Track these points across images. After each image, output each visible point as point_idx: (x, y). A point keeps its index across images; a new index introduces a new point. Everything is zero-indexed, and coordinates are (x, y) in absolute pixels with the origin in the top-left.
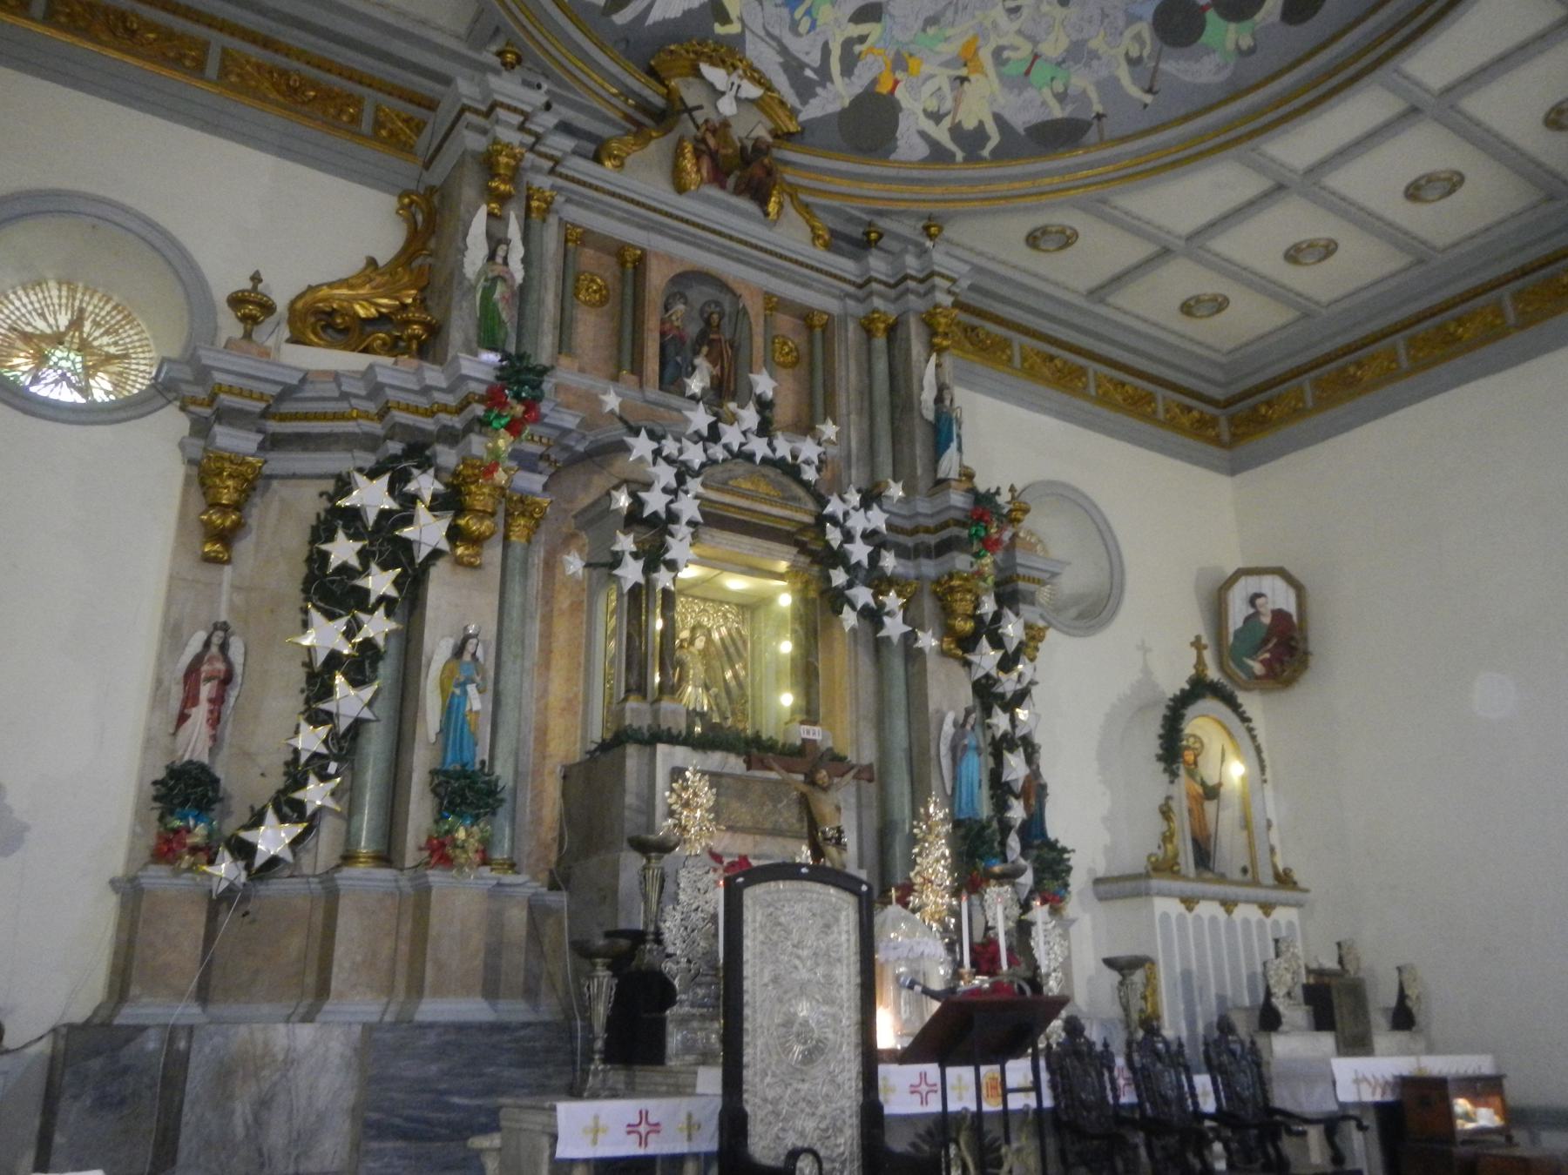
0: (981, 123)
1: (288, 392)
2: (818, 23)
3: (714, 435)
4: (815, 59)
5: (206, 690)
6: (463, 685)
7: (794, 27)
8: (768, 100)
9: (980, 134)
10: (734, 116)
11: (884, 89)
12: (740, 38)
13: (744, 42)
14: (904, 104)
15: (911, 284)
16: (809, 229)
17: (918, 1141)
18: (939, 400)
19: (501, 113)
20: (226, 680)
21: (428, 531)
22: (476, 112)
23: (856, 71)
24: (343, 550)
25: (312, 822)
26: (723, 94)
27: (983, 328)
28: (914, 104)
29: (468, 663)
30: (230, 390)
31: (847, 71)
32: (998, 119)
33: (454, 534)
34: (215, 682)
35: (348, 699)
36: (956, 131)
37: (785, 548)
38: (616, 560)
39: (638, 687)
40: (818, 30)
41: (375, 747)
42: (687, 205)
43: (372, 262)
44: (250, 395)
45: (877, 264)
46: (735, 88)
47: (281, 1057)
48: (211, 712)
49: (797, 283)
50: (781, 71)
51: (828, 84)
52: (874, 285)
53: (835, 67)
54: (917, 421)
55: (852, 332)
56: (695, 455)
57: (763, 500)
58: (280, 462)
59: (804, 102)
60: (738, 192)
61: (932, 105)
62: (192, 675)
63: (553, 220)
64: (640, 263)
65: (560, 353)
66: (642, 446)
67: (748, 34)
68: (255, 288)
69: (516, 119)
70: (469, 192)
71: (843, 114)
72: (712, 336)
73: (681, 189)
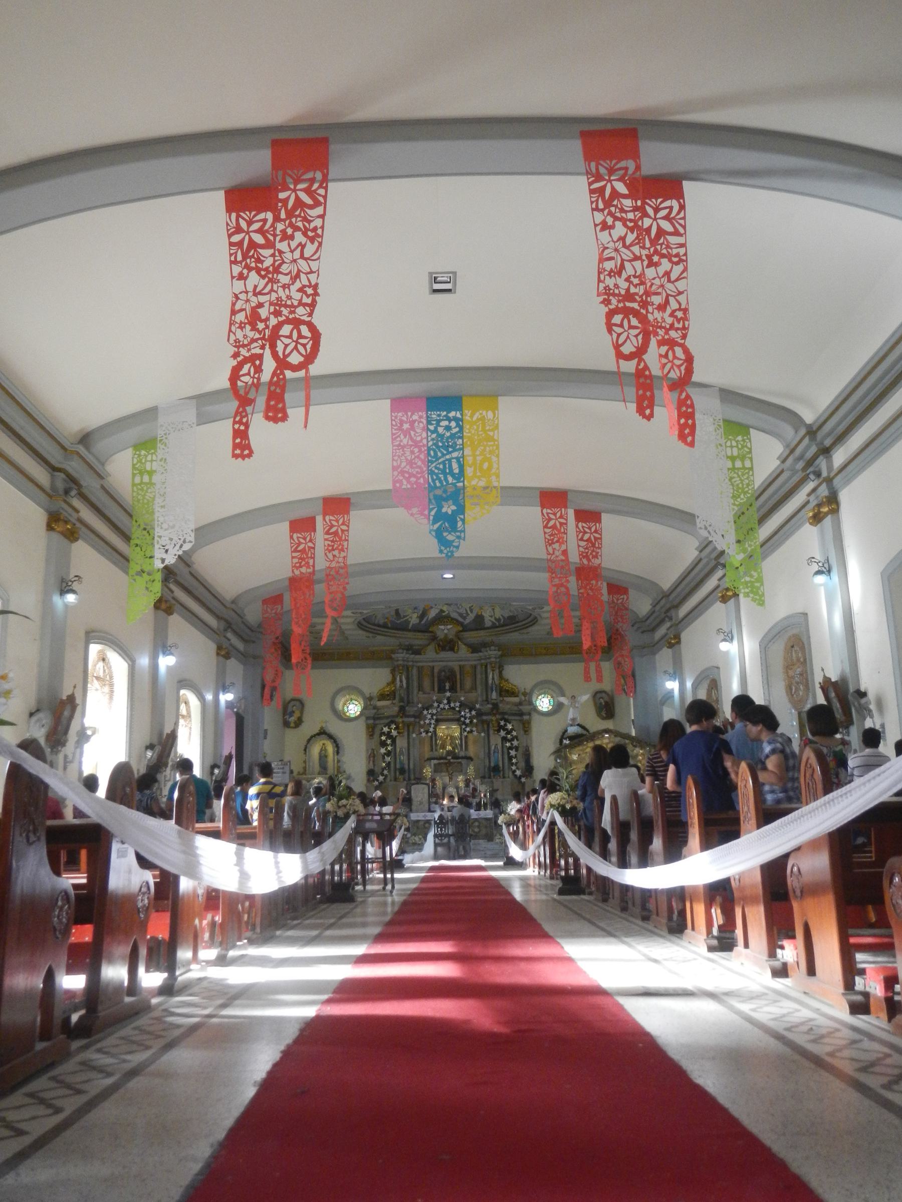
1: (375, 713)
3: (439, 706)
4: (465, 612)
7: (458, 608)
20: (374, 757)
21: (394, 733)
24: (383, 738)
25: (386, 776)
28: (487, 614)
33: (398, 733)
35: (388, 759)
36: (496, 619)
38: (421, 733)
39: (432, 750)
41: (392, 765)
45: (481, 654)
53: (469, 612)
56: (435, 711)
58: (377, 722)
62: (369, 757)
66: (425, 712)
70: (397, 673)
73: (437, 653)
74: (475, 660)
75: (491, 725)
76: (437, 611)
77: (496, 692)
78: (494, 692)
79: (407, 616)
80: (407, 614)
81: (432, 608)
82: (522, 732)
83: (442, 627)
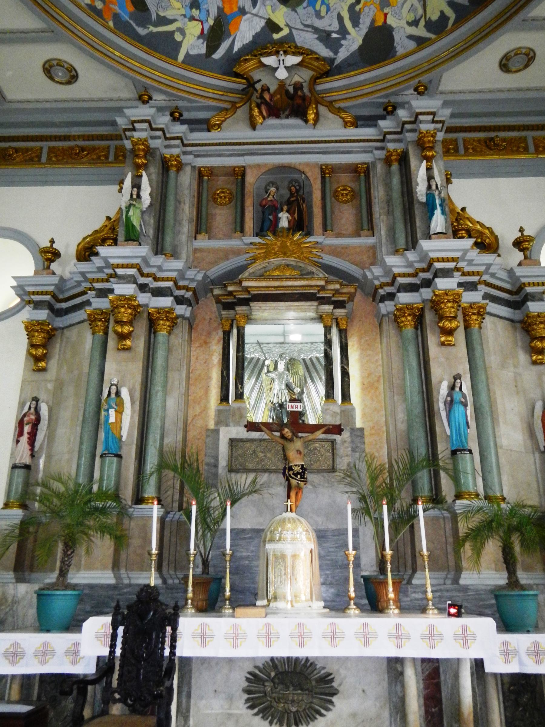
0: (442, 12)
2: (330, 5)
4: (335, 26)
5: (27, 429)
6: (107, 410)
8: (307, 60)
9: (443, 17)
10: (287, 78)
11: (380, 23)
12: (291, 33)
13: (293, 36)
14: (394, 25)
15: (407, 126)
16: (341, 120)
17: (257, 672)
18: (429, 187)
19: (137, 125)
20: (36, 424)
22: (129, 130)
23: (361, 21)
26: (276, 69)
27: (497, 136)
29: (112, 399)
30: (33, 293)
31: (356, 23)
32: (451, 4)
34: (30, 425)
36: (430, 26)
37: (309, 303)
40: (332, 9)
42: (260, 135)
43: (108, 218)
44: (42, 293)
45: (386, 124)
46: (281, 62)
47: (10, 600)
48: (29, 438)
49: (343, 153)
50: (317, 42)
51: (347, 36)
52: (388, 137)
53: (348, 24)
54: (416, 206)
55: (380, 168)
57: (287, 279)
59: (336, 53)
60: (287, 117)
61: (411, 18)
62: (21, 424)
63: (188, 169)
64: (243, 175)
65: (198, 231)
67: (294, 31)
68: (52, 246)
69: (145, 126)
71: (360, 47)
72: (292, 199)
73: (253, 126)
74: (371, 152)
75: (429, 317)
76: (259, 25)
77: (443, 213)
78: (438, 212)
79: (171, 22)
80: (169, 14)
81: (243, 12)
82: (523, 357)
83: (269, 61)
